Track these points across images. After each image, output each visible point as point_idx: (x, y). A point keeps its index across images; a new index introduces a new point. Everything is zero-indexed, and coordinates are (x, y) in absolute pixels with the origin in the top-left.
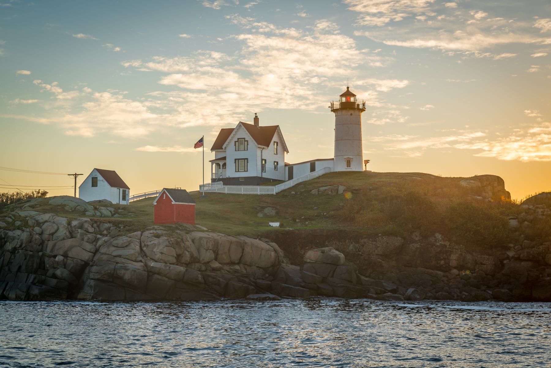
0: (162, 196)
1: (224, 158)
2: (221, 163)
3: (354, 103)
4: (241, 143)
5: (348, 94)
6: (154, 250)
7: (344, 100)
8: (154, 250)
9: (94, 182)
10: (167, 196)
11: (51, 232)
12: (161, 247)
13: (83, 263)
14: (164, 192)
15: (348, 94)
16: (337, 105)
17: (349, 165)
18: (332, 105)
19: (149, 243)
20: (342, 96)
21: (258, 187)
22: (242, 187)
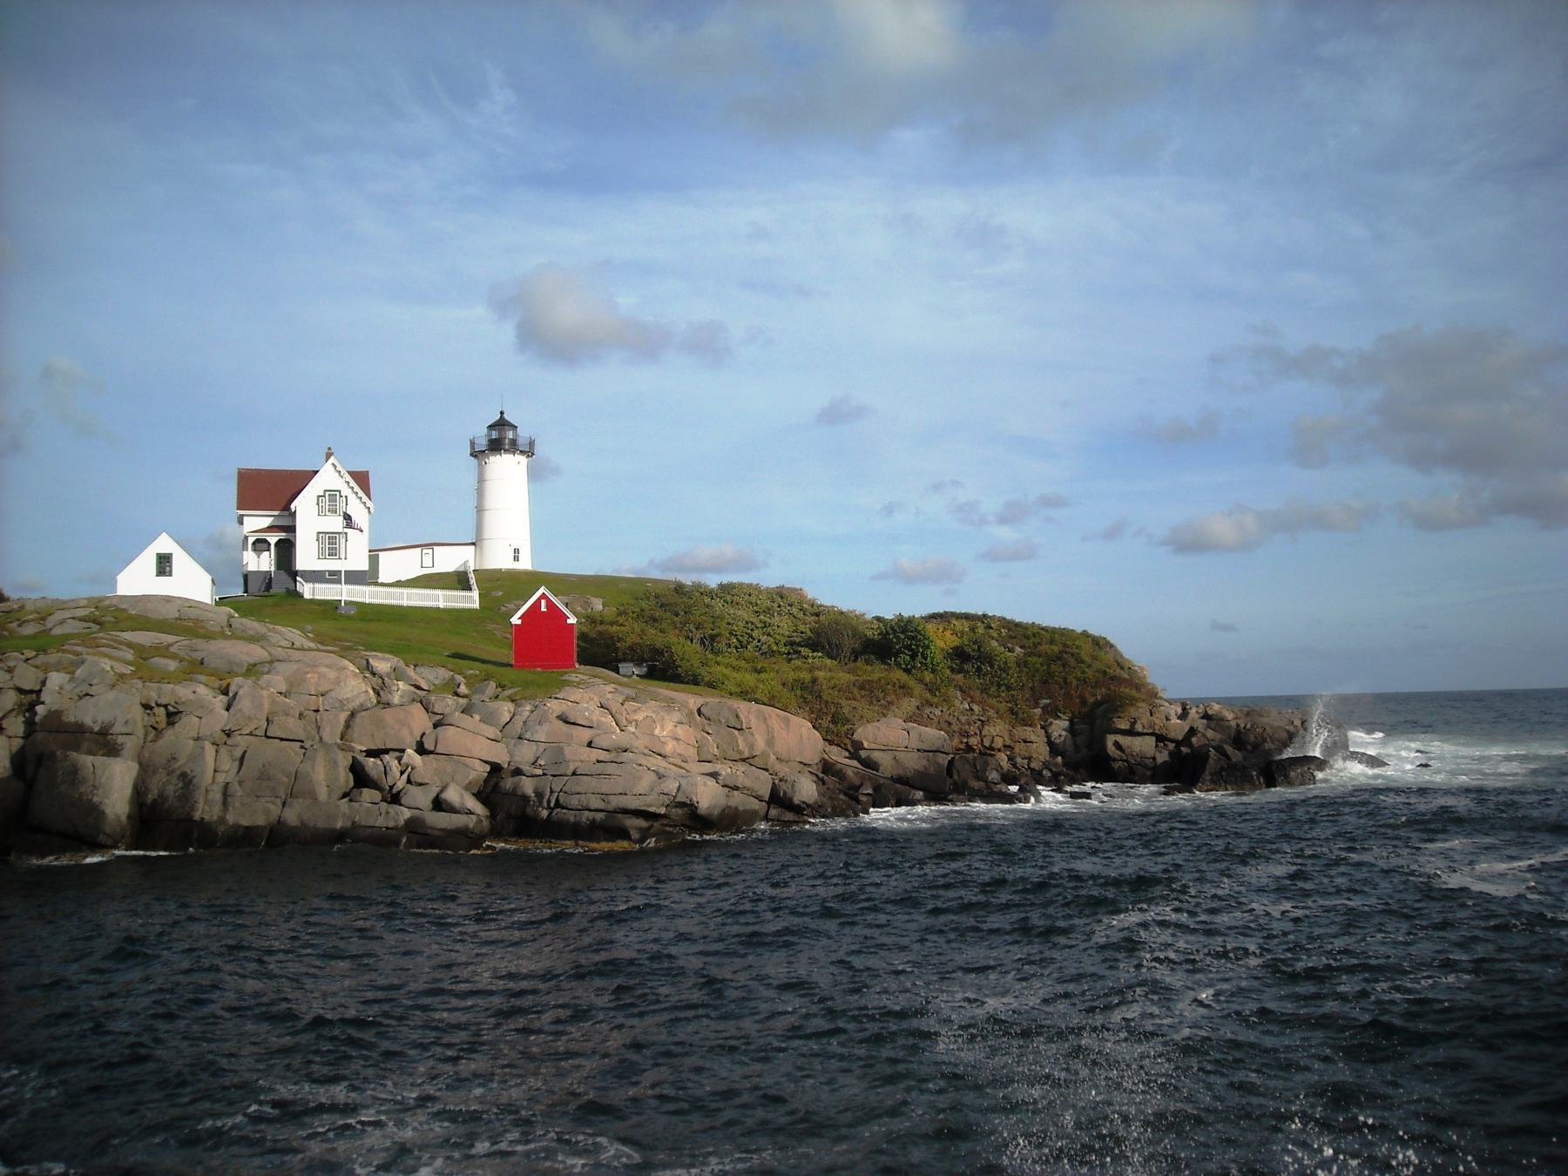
0: (538, 601)
1: (291, 529)
2: (273, 539)
3: (514, 442)
4: (331, 500)
5: (501, 424)
6: (657, 732)
7: (494, 435)
8: (657, 732)
9: (164, 565)
10: (550, 604)
11: (322, 689)
12: (669, 726)
13: (488, 768)
14: (543, 596)
15: (501, 424)
16: (482, 443)
17: (516, 559)
18: (472, 444)
19: (640, 716)
20: (491, 427)
21: (440, 593)
22: (406, 591)
